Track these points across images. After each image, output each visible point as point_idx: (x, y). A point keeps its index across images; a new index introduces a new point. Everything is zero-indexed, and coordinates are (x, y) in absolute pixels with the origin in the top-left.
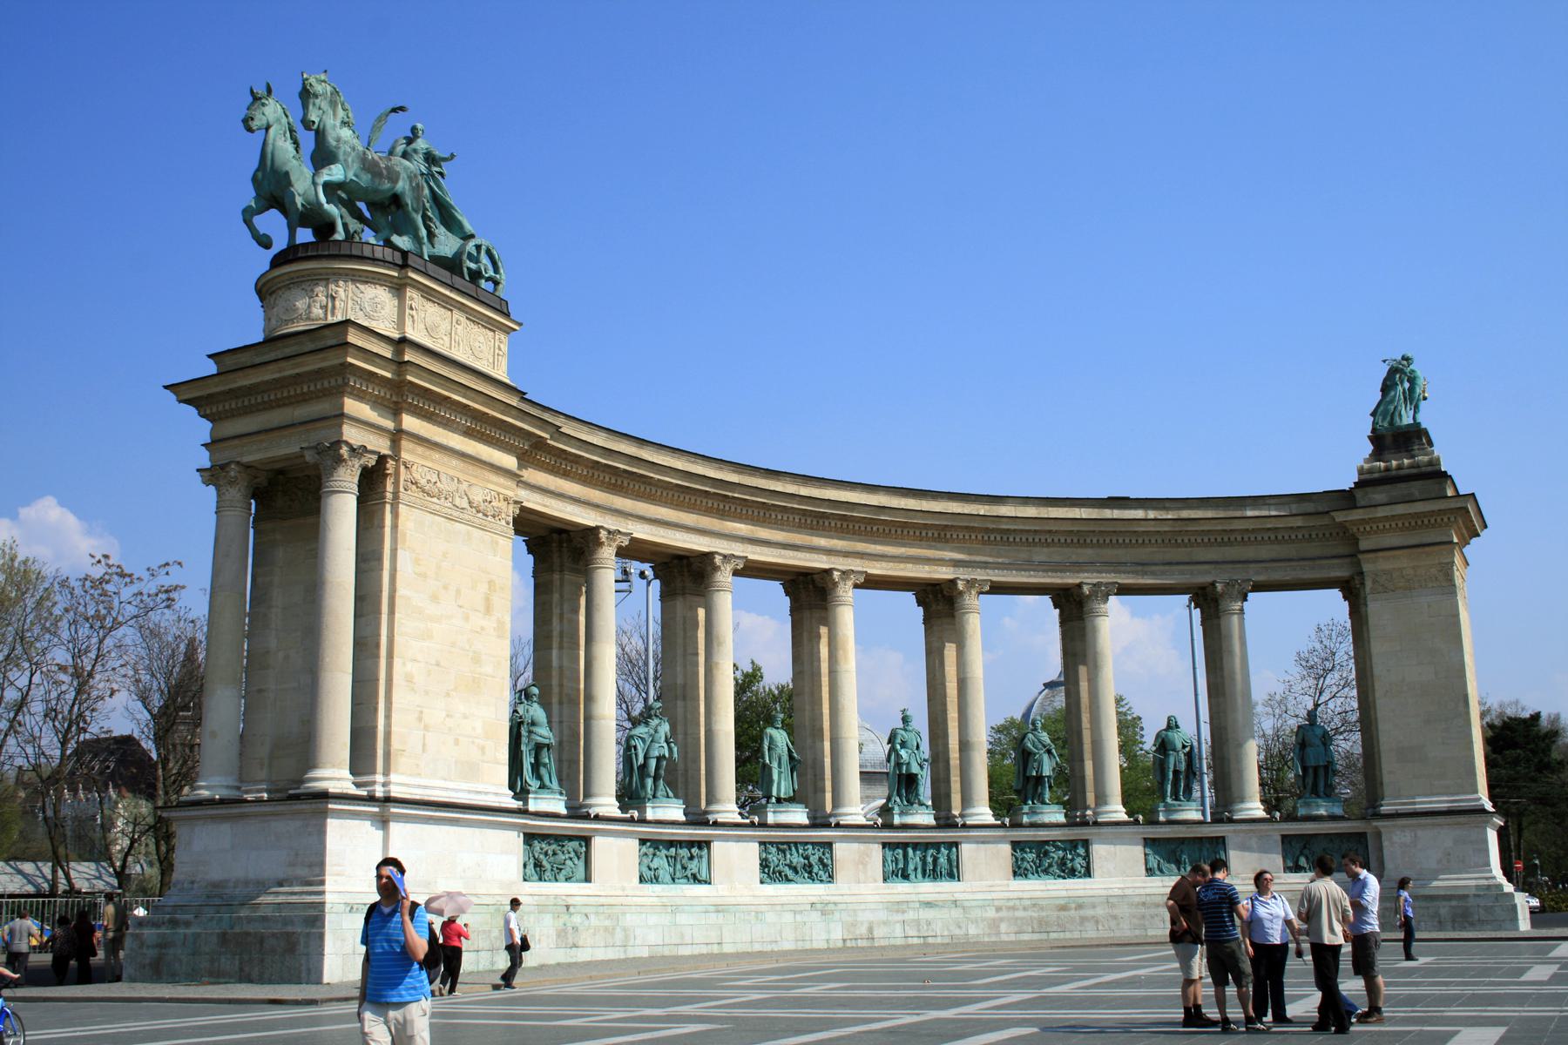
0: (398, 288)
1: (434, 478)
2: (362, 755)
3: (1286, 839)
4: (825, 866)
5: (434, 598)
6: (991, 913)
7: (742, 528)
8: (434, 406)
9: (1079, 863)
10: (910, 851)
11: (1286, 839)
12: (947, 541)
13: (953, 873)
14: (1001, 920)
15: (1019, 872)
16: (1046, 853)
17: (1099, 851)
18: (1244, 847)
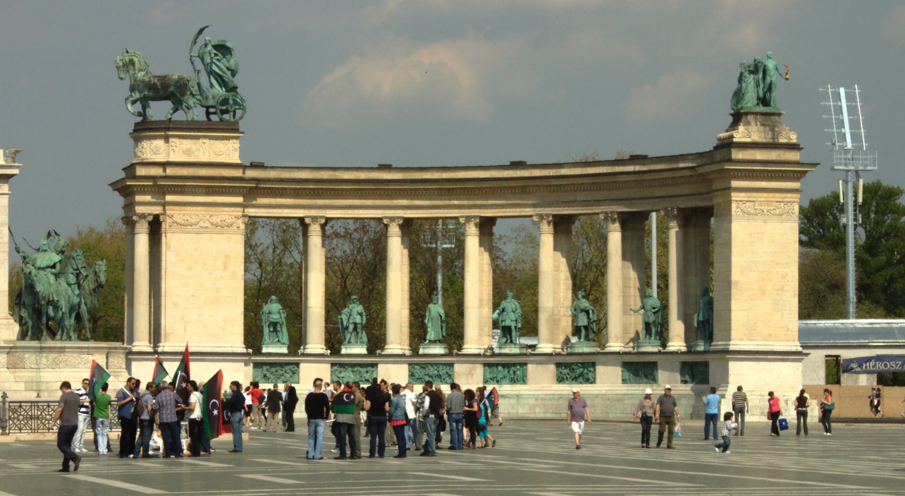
0: (167, 139)
1: (188, 218)
2: (156, 335)
3: (684, 365)
4: (449, 376)
5: (190, 269)
6: (532, 402)
9: (590, 375)
10: (500, 368)
11: (684, 365)
12: (529, 193)
13: (523, 380)
14: (537, 406)
15: (560, 380)
16: (573, 369)
17: (600, 369)
18: (664, 369)
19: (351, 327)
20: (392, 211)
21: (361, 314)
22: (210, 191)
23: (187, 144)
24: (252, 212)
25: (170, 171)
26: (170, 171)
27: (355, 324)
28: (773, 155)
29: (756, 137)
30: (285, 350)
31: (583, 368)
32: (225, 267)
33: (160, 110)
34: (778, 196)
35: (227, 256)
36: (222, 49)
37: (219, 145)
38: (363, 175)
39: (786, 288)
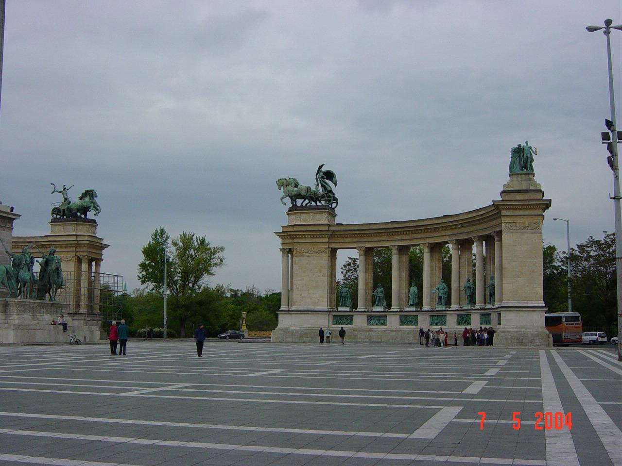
7: (398, 237)
8: (297, 237)
13: (444, 324)
15: (459, 323)
19: (378, 298)
20: (394, 243)
21: (382, 292)
22: (313, 237)
23: (304, 216)
24: (334, 246)
25: (296, 229)
26: (296, 229)
27: (380, 297)
28: (526, 196)
29: (516, 188)
30: (348, 309)
31: (467, 317)
32: (320, 271)
33: (299, 202)
34: (530, 219)
35: (321, 267)
36: (329, 175)
37: (318, 216)
38: (381, 227)
39: (535, 271)
